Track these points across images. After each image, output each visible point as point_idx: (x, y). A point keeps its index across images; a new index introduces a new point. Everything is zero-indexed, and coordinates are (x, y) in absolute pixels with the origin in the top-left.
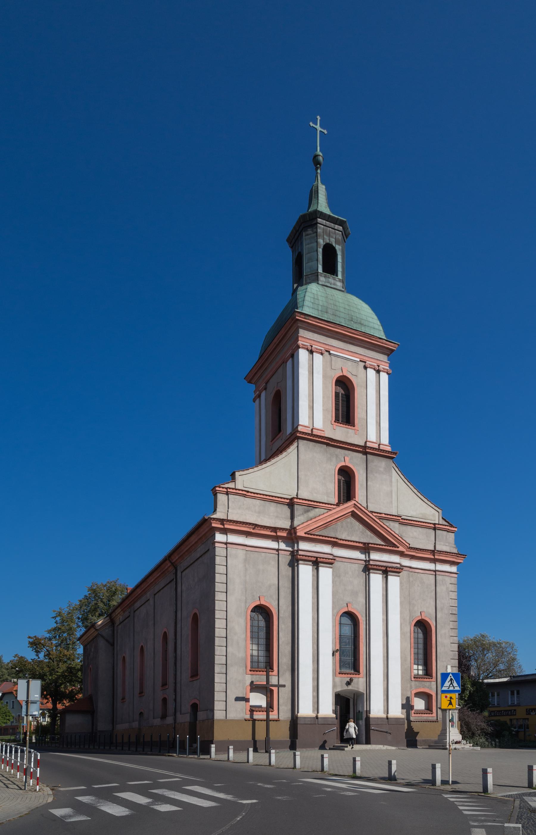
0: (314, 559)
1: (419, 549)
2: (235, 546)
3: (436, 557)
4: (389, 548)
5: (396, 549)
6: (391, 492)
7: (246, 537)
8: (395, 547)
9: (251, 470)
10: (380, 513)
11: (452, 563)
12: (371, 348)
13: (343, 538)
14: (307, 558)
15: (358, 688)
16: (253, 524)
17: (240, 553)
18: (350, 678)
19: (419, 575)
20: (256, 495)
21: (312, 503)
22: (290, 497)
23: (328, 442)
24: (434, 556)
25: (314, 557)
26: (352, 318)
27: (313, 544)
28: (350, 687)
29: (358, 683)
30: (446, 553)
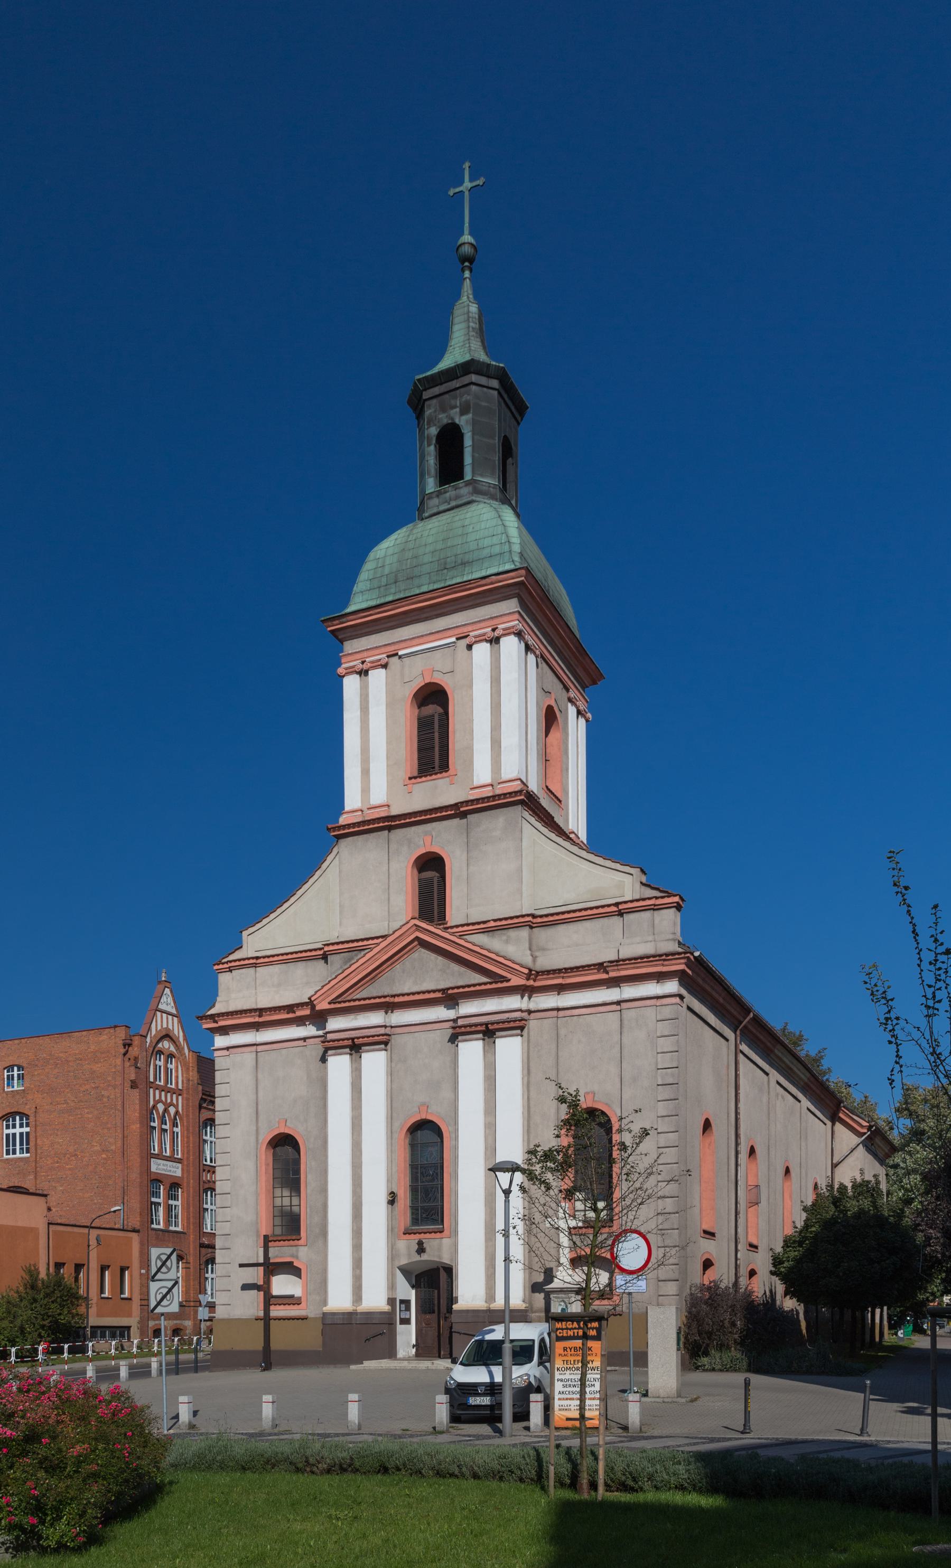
0: (350, 1042)
1: (565, 969)
2: (240, 1049)
3: (613, 974)
4: (494, 986)
5: (505, 984)
6: (520, 870)
7: (257, 1031)
8: (502, 982)
9: (265, 921)
10: (484, 922)
11: (660, 977)
12: (478, 601)
13: (406, 990)
14: (336, 1044)
15: (440, 1257)
16: (255, 1010)
17: (248, 1057)
18: (417, 1241)
19: (581, 1019)
20: (271, 959)
21: (355, 944)
22: (319, 945)
23: (386, 824)
24: (607, 973)
25: (348, 1039)
26: (445, 563)
27: (352, 1016)
28: (425, 1257)
29: (440, 1248)
30: (633, 961)
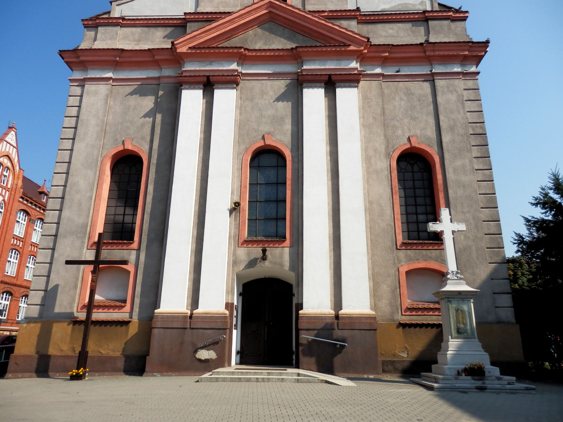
25: (204, 76)
